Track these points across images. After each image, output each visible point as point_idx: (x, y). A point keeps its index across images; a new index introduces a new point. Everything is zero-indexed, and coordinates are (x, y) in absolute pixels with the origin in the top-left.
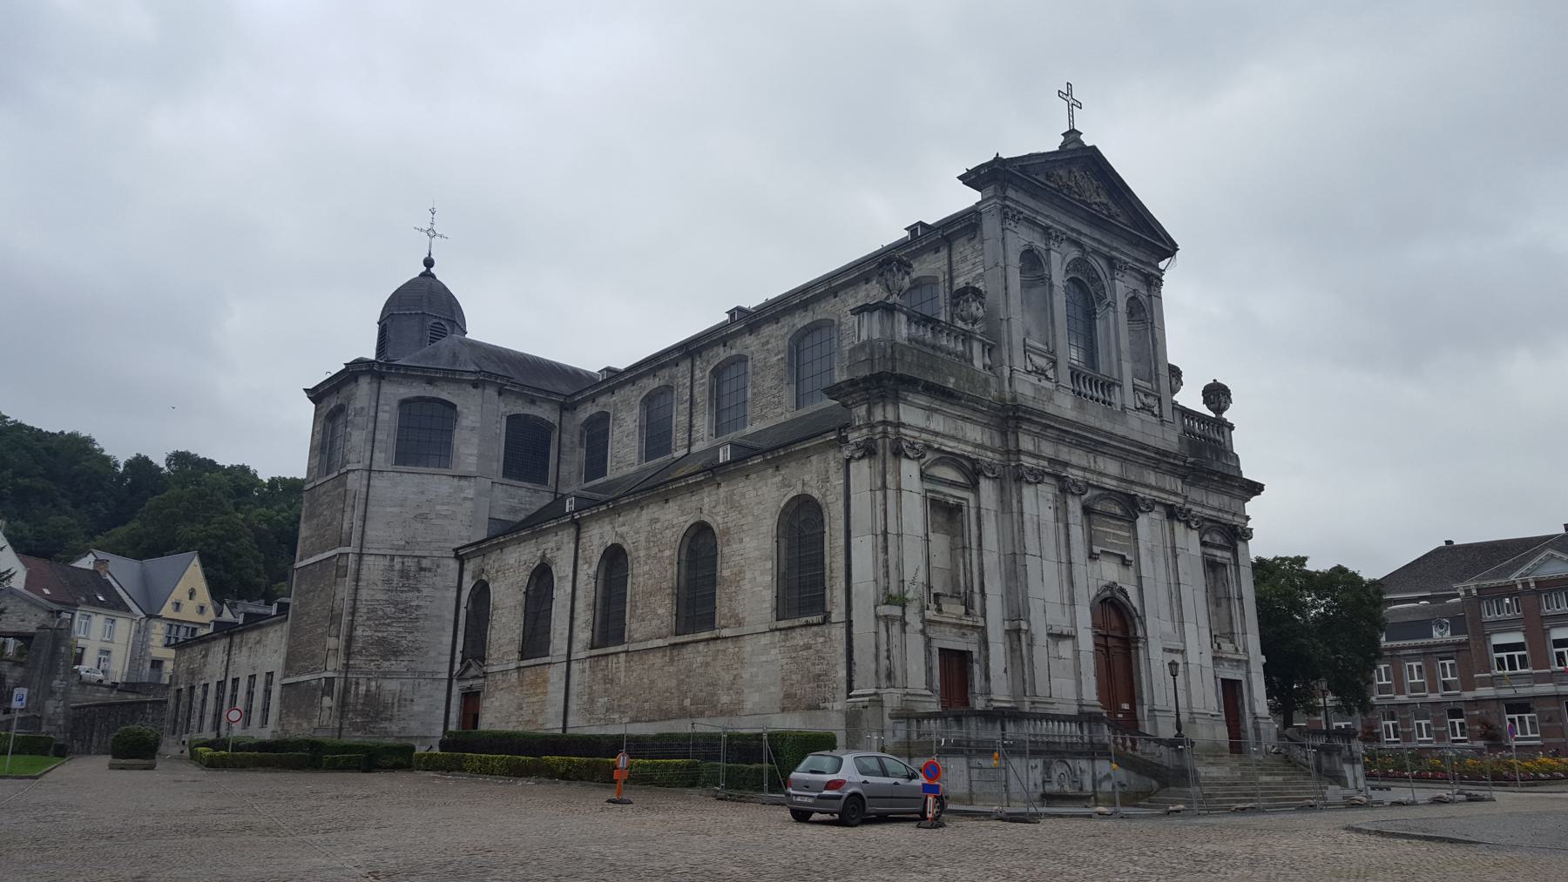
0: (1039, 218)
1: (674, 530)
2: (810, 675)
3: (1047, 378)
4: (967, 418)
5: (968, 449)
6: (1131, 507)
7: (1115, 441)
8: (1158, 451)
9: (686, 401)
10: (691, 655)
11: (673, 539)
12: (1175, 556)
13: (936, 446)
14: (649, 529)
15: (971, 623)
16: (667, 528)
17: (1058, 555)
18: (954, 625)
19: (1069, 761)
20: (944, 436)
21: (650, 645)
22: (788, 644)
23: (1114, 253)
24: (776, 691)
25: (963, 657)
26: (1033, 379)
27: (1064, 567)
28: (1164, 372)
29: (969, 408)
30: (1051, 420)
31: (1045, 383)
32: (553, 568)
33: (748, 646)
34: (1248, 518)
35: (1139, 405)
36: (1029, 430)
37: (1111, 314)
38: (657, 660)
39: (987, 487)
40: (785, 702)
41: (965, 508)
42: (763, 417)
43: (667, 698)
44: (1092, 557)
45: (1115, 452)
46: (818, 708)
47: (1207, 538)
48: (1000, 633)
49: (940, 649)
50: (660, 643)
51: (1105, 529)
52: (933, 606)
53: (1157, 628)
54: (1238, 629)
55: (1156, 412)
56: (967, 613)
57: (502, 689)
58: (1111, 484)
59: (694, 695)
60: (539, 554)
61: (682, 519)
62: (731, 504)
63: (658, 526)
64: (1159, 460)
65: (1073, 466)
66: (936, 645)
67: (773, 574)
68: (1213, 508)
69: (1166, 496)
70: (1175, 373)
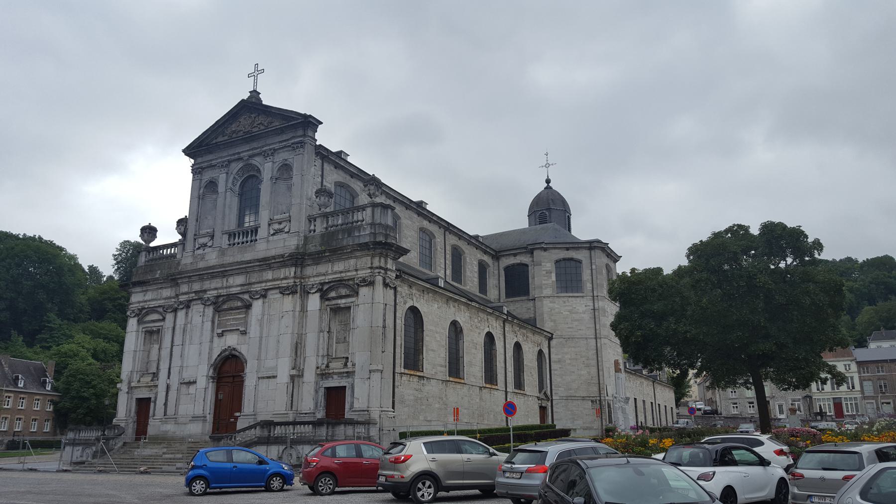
0: (213, 162)
7: (229, 267)
8: (259, 260)
13: (146, 307)
15: (152, 384)
18: (146, 387)
20: (149, 301)
29: (155, 284)
30: (187, 274)
36: (183, 282)
39: (169, 317)
51: (227, 318)
65: (209, 290)
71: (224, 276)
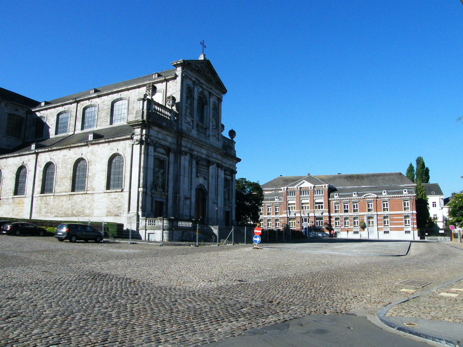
1: (72, 159)
2: (116, 206)
3: (190, 125)
4: (168, 135)
5: (168, 144)
6: (209, 163)
9: (74, 117)
10: (76, 198)
11: (71, 162)
12: (218, 178)
13: (159, 143)
14: (63, 158)
16: (69, 158)
17: (189, 176)
19: (188, 232)
21: (62, 194)
22: (109, 197)
23: (211, 91)
24: (105, 211)
25: (161, 203)
26: (187, 125)
27: (190, 179)
28: (220, 126)
31: (190, 126)
32: (27, 167)
33: (96, 196)
34: (236, 168)
35: (213, 135)
37: (208, 108)
38: (64, 199)
40: (108, 213)
41: (165, 162)
42: (101, 125)
43: (68, 210)
44: (197, 176)
45: (206, 148)
46: (118, 216)
47: (226, 173)
48: (171, 197)
49: (155, 201)
50: (66, 194)
52: (154, 189)
53: (211, 196)
54: (230, 197)
55: (217, 137)
56: (163, 191)
57: (6, 204)
58: (204, 156)
59: (77, 210)
60: (22, 162)
61: (75, 156)
62: (92, 152)
63: (66, 157)
64: (216, 150)
66: (155, 199)
67: (106, 176)
68: (228, 165)
69: (217, 161)
70: (223, 126)
71: (200, 147)
